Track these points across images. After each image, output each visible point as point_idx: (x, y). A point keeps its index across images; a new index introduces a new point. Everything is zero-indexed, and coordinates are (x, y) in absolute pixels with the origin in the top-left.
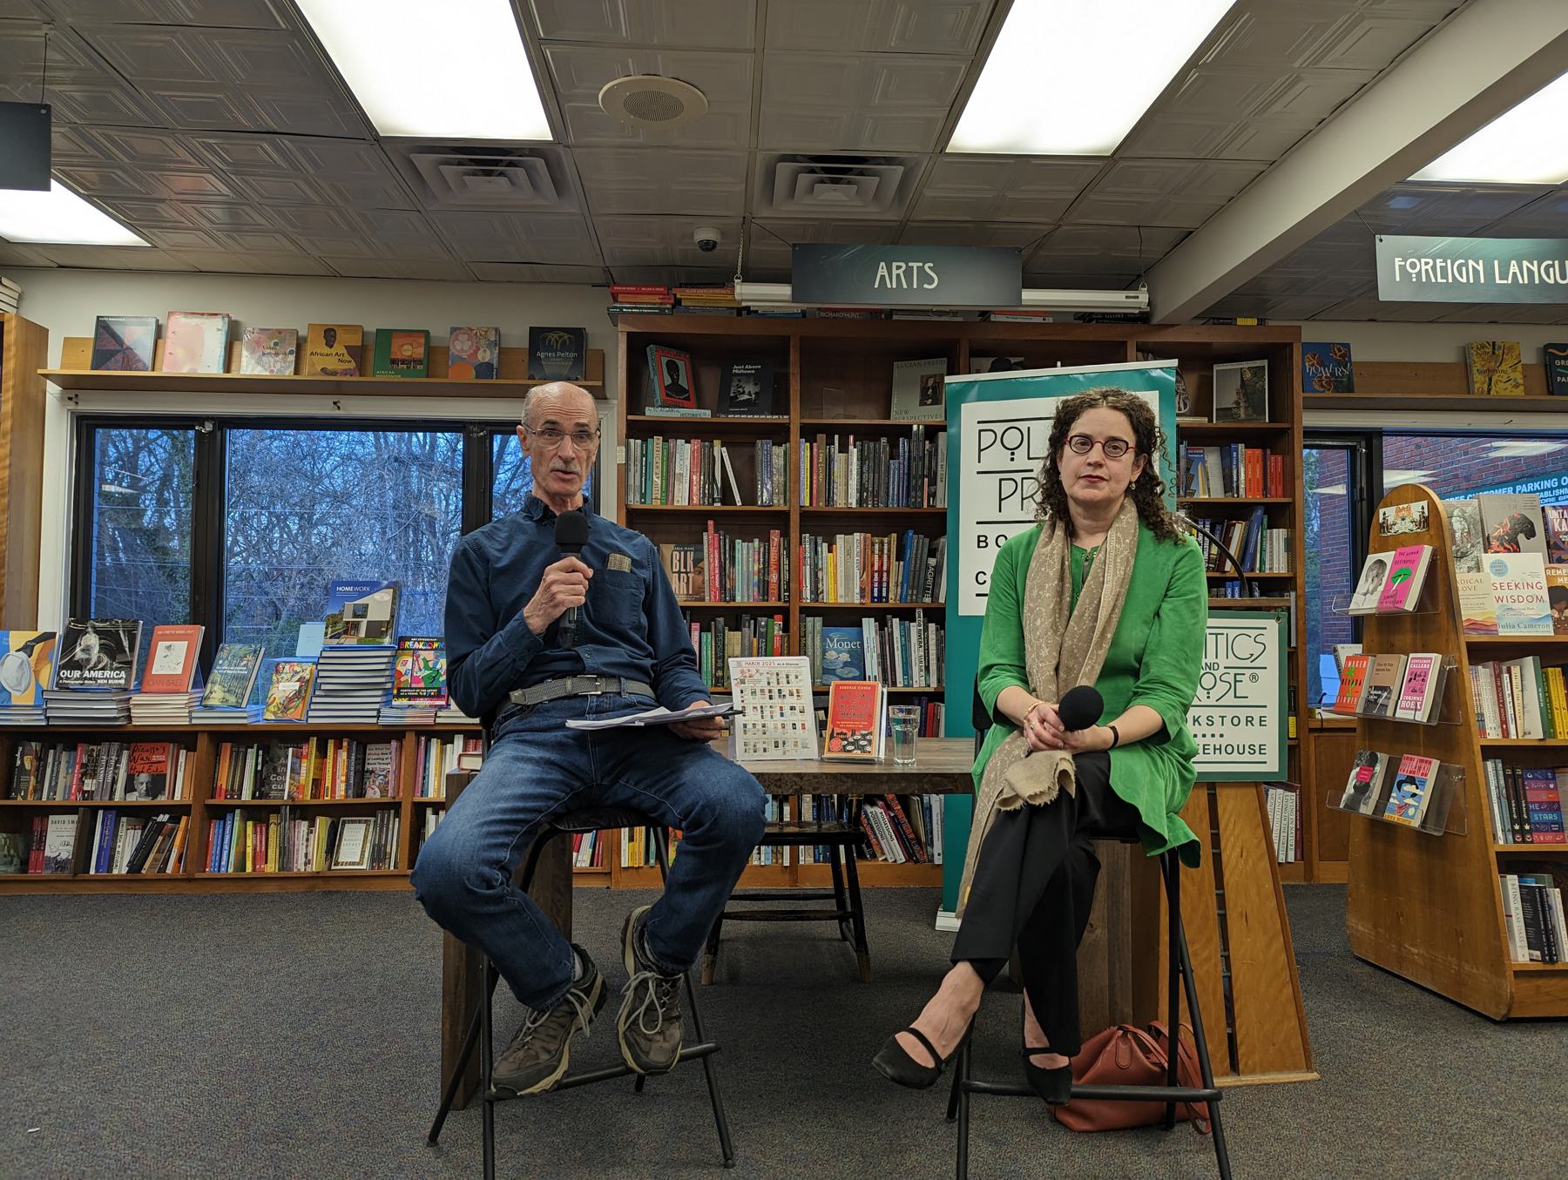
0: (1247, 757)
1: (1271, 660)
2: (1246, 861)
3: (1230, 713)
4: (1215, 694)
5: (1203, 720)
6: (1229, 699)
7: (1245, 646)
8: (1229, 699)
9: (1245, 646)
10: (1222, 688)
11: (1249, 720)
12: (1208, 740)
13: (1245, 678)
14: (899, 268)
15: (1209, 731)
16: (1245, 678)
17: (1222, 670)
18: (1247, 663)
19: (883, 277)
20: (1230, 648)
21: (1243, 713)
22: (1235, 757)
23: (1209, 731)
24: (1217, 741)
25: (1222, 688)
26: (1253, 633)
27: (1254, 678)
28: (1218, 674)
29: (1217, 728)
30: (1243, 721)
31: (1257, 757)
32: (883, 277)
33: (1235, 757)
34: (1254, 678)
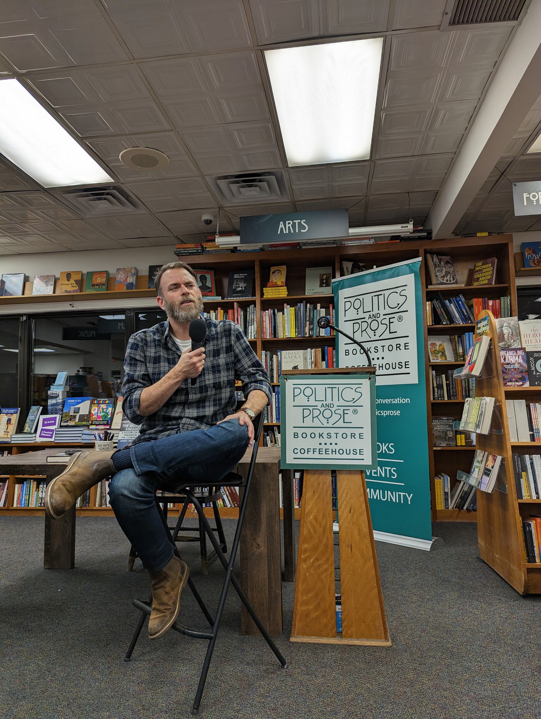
0: (351, 456)
1: (366, 401)
2: (353, 515)
4: (332, 421)
5: (325, 435)
6: (340, 424)
7: (349, 394)
8: (340, 424)
9: (349, 394)
10: (335, 417)
11: (353, 436)
13: (350, 412)
14: (289, 223)
15: (328, 441)
16: (350, 412)
18: (351, 404)
19: (282, 228)
20: (340, 395)
21: (349, 432)
22: (345, 456)
23: (328, 441)
24: (334, 447)
25: (335, 417)
26: (354, 387)
27: (355, 412)
28: (333, 410)
29: (333, 440)
30: (349, 436)
31: (358, 456)
32: (282, 228)
33: (345, 456)
34: (355, 412)
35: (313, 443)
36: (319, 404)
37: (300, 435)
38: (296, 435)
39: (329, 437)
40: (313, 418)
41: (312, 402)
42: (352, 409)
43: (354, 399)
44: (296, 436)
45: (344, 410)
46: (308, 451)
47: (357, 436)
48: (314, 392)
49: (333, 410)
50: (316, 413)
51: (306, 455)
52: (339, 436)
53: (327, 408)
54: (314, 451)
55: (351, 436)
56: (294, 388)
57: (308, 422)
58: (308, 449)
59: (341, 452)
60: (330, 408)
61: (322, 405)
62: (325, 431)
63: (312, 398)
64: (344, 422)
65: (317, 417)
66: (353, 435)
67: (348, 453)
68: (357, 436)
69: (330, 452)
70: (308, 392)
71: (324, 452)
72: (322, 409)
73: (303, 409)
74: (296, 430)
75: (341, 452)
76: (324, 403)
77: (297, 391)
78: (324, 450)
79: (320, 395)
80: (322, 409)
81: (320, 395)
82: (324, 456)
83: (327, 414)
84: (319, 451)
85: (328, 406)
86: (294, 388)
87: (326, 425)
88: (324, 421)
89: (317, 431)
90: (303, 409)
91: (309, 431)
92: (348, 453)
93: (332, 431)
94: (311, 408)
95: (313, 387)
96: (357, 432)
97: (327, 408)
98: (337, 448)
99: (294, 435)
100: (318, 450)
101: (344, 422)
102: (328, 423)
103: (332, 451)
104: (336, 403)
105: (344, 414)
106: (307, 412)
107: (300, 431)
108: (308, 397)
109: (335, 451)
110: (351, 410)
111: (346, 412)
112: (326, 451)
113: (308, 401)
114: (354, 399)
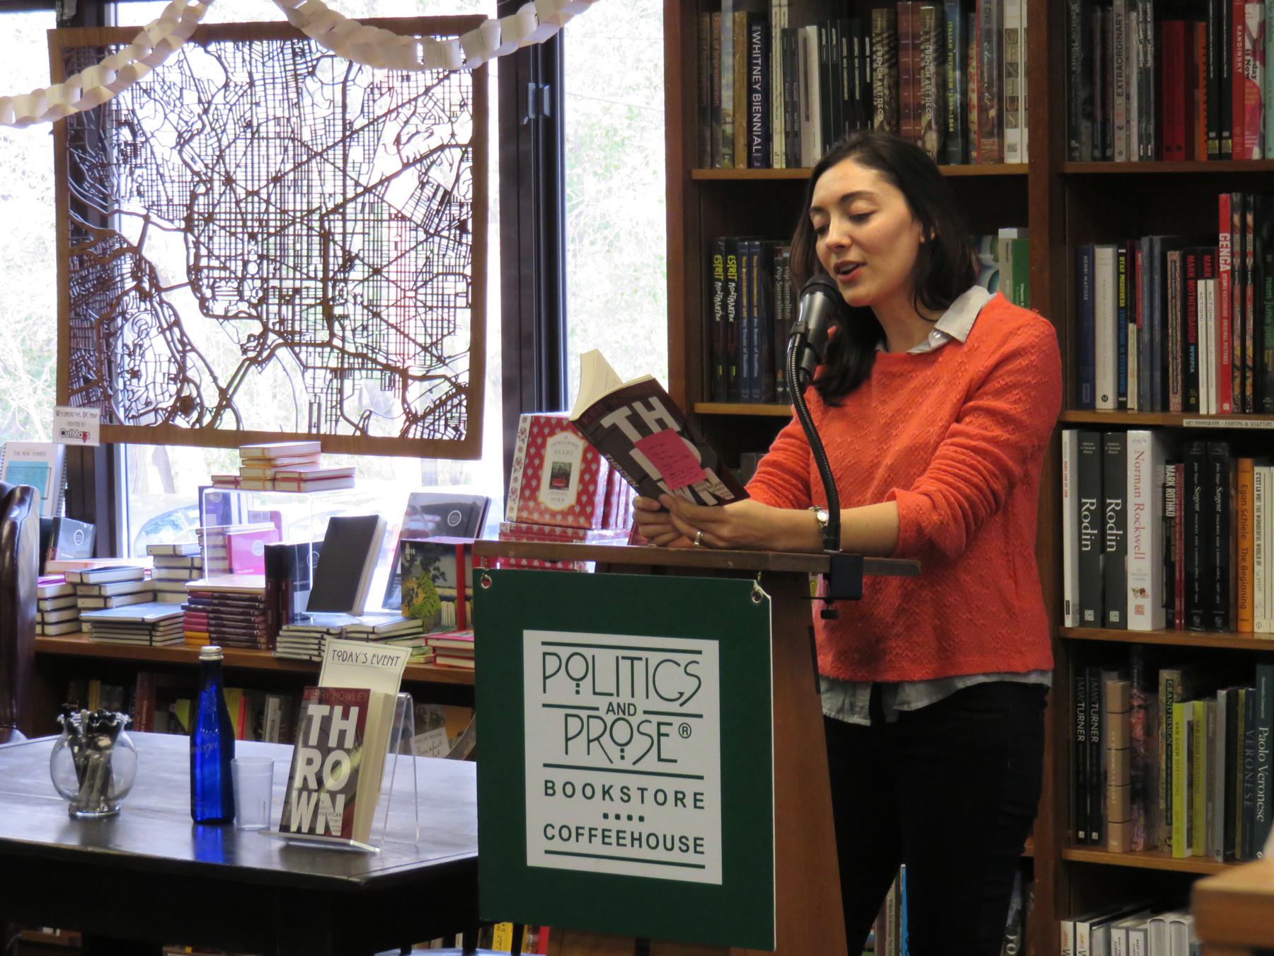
3: (653, 783)
4: (633, 752)
5: (616, 793)
7: (672, 680)
9: (672, 680)
10: (640, 744)
11: (679, 798)
12: (623, 824)
13: (673, 731)
15: (624, 810)
17: (640, 717)
18: (674, 707)
21: (671, 785)
22: (660, 854)
24: (635, 826)
25: (640, 744)
27: (685, 731)
28: (635, 723)
29: (634, 807)
34: (685, 731)
35: (586, 813)
36: (602, 702)
37: (558, 788)
38: (549, 788)
39: (626, 798)
40: (589, 741)
42: (677, 721)
43: (682, 694)
44: (550, 791)
45: (659, 724)
46: (578, 834)
47: (689, 800)
49: (635, 721)
50: (596, 728)
51: (571, 846)
52: (649, 795)
53: (621, 715)
54: (591, 836)
55: (676, 799)
57: (578, 752)
58: (577, 828)
59: (653, 841)
60: (626, 717)
61: (610, 709)
62: (617, 781)
64: (660, 759)
65: (597, 739)
66: (680, 796)
67: (669, 846)
68: (689, 800)
69: (628, 841)
71: (613, 840)
72: (610, 718)
73: (567, 716)
74: (552, 774)
75: (653, 841)
76: (614, 700)
78: (613, 834)
79: (605, 682)
80: (610, 718)
81: (605, 682)
82: (614, 850)
83: (621, 732)
84: (604, 837)
85: (623, 712)
87: (618, 764)
88: (614, 752)
89: (599, 780)
90: (567, 716)
91: (579, 778)
92: (669, 846)
93: (633, 782)
94: (584, 714)
96: (689, 787)
97: (621, 715)
98: (645, 829)
99: (547, 788)
100: (599, 833)
101: (660, 759)
102: (622, 758)
103: (633, 839)
104: (642, 703)
105: (660, 735)
106: (574, 725)
107: (559, 777)
109: (640, 839)
110: (676, 726)
111: (664, 729)
112: (618, 838)
113: (578, 692)
114: (682, 694)
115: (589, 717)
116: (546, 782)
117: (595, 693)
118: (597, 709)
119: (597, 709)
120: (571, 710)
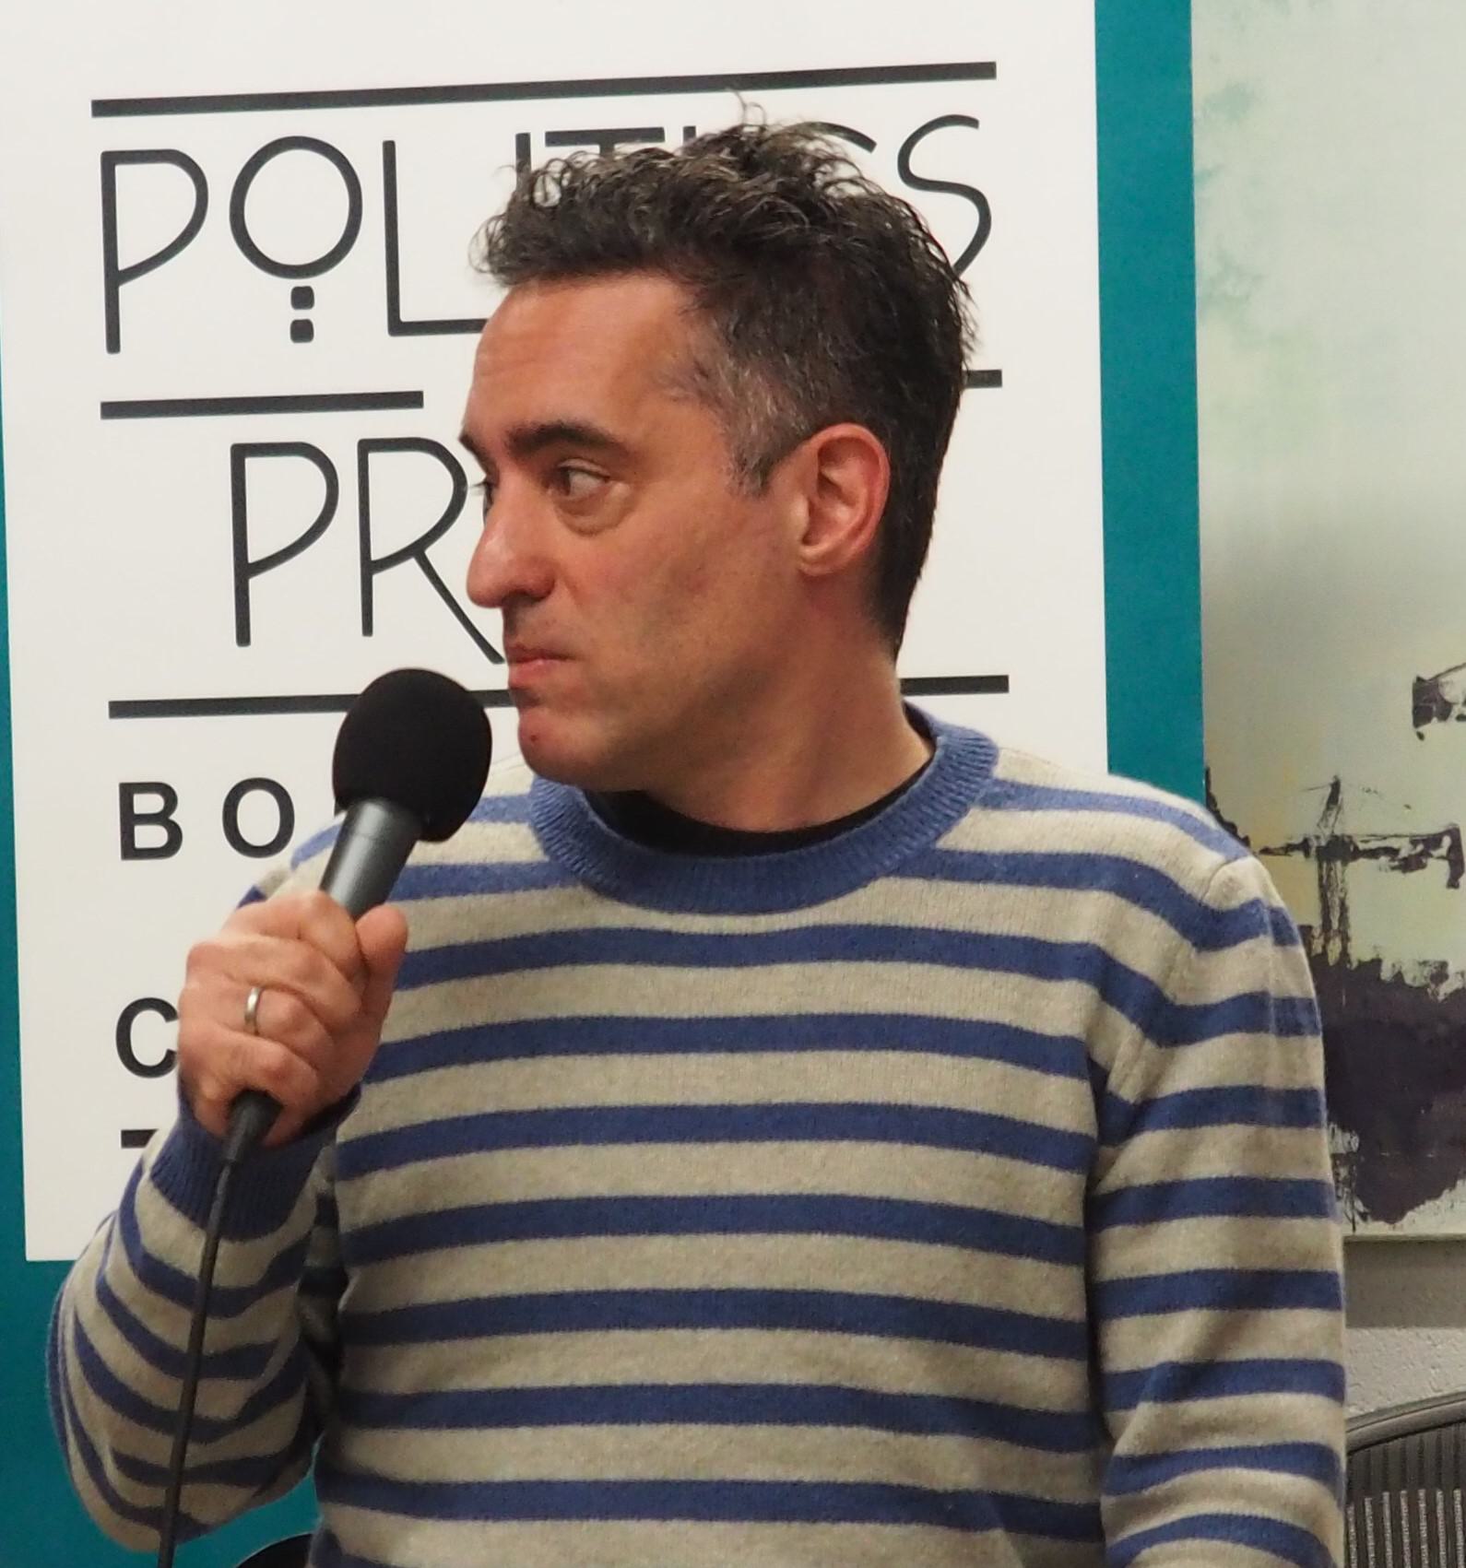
37: (199, 818)
40: (370, 567)
41: (353, 349)
44: (151, 836)
48: (375, 204)
56: (111, 160)
63: (350, 294)
65: (417, 550)
70: (298, 209)
73: (241, 453)
77: (153, 203)
86: (111, 160)
90: (241, 453)
94: (338, 434)
95: (357, 133)
99: (130, 820)
106: (285, 497)
108: (302, 278)
113: (302, 331)
115: (366, 447)
116: (128, 791)
117: (398, 327)
118: (412, 400)
119: (412, 400)
120: (258, 422)
